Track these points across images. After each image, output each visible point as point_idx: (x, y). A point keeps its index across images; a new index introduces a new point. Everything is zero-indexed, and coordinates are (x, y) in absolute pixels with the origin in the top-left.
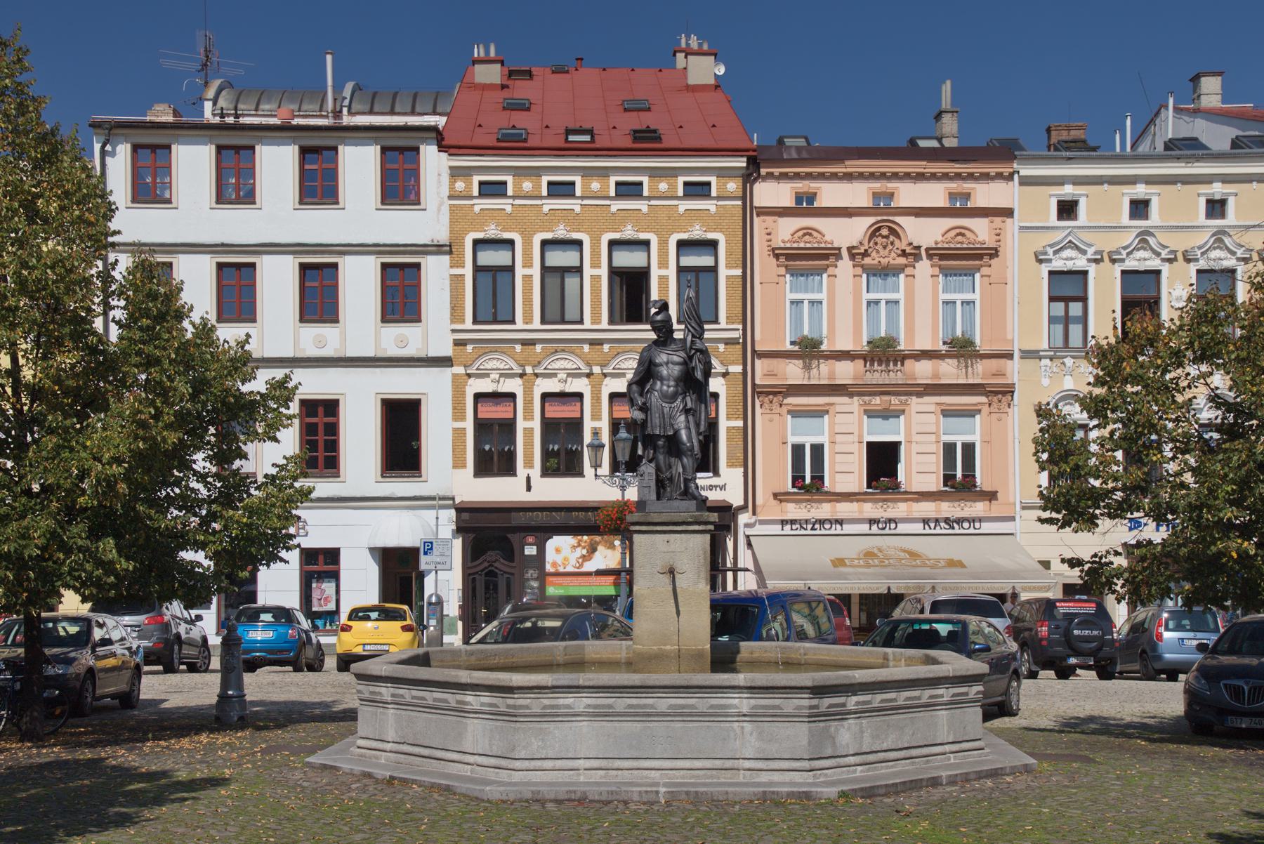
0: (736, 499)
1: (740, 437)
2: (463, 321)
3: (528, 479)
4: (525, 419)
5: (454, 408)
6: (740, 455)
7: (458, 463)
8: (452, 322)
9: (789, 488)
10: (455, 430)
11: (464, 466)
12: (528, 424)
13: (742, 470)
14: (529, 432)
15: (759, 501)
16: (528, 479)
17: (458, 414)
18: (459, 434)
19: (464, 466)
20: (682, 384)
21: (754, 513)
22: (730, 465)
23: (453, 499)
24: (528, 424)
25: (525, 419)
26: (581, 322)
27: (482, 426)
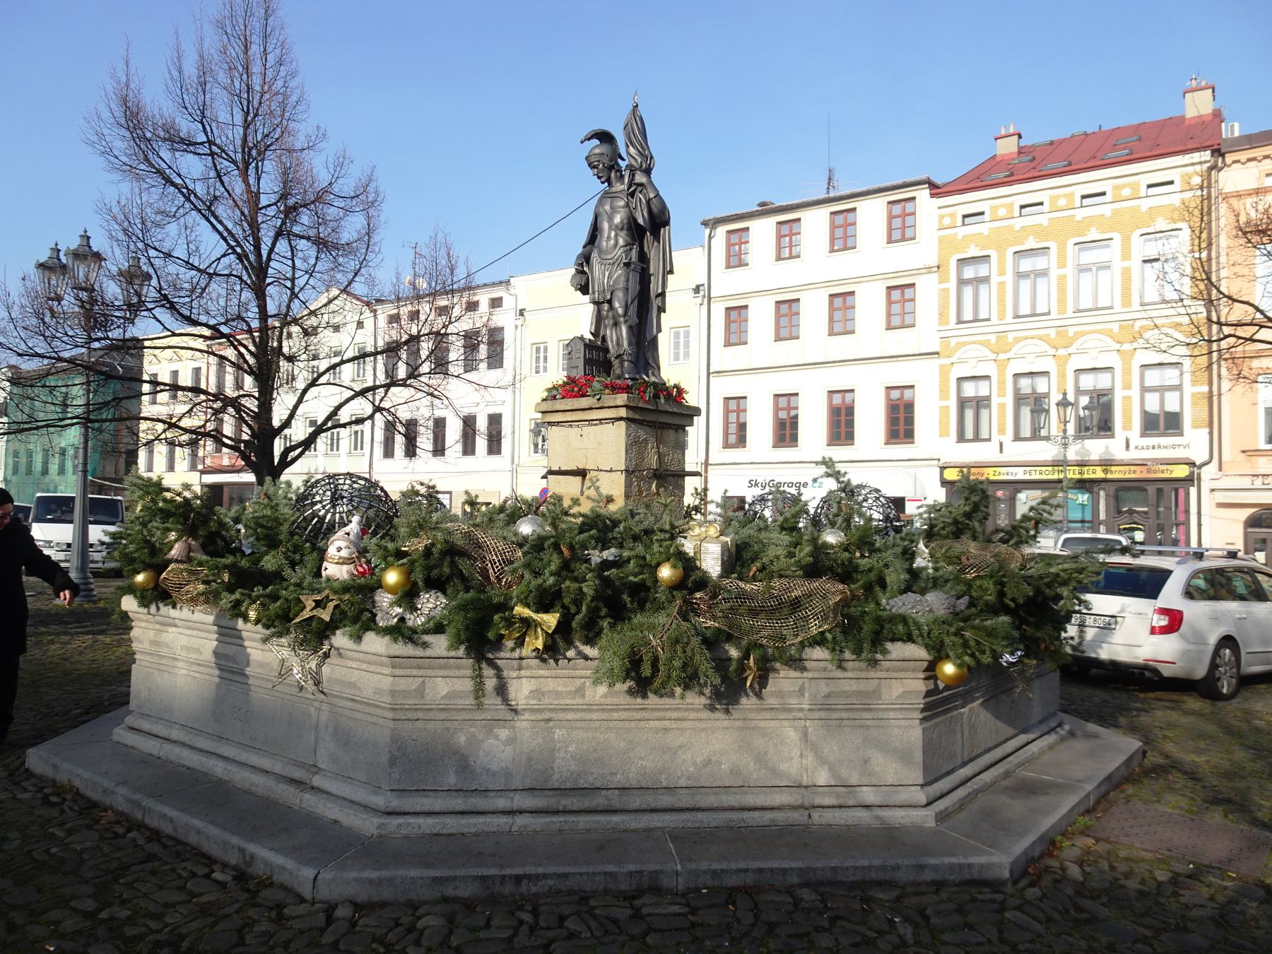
0: (1200, 456)
1: (1206, 401)
2: (948, 323)
3: (1001, 444)
4: (999, 396)
5: (941, 391)
6: (1205, 415)
7: (944, 433)
8: (940, 325)
9: (1263, 445)
10: (941, 407)
11: (948, 435)
12: (1002, 400)
13: (1207, 430)
14: (1002, 406)
15: (1226, 457)
16: (1001, 444)
17: (944, 394)
18: (945, 411)
19: (948, 435)
20: (623, 234)
21: (1220, 469)
22: (1196, 426)
23: (939, 460)
24: (1002, 400)
25: (999, 396)
26: (1049, 313)
27: (963, 403)
